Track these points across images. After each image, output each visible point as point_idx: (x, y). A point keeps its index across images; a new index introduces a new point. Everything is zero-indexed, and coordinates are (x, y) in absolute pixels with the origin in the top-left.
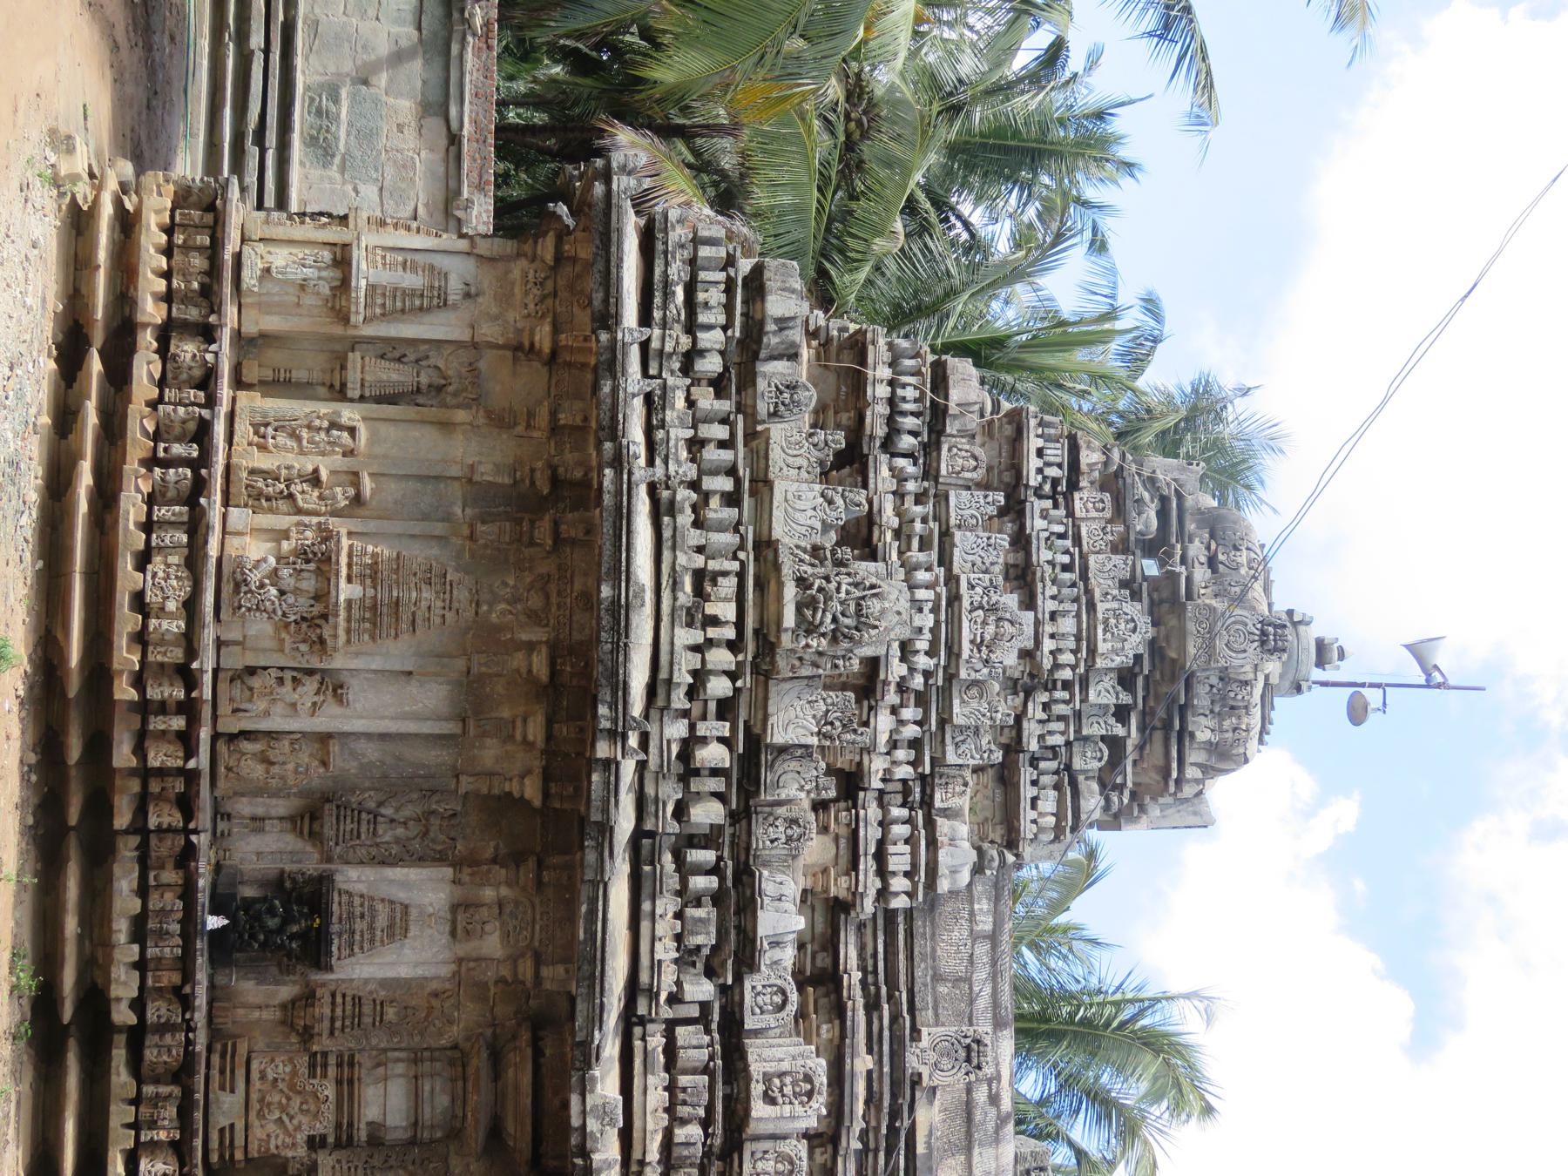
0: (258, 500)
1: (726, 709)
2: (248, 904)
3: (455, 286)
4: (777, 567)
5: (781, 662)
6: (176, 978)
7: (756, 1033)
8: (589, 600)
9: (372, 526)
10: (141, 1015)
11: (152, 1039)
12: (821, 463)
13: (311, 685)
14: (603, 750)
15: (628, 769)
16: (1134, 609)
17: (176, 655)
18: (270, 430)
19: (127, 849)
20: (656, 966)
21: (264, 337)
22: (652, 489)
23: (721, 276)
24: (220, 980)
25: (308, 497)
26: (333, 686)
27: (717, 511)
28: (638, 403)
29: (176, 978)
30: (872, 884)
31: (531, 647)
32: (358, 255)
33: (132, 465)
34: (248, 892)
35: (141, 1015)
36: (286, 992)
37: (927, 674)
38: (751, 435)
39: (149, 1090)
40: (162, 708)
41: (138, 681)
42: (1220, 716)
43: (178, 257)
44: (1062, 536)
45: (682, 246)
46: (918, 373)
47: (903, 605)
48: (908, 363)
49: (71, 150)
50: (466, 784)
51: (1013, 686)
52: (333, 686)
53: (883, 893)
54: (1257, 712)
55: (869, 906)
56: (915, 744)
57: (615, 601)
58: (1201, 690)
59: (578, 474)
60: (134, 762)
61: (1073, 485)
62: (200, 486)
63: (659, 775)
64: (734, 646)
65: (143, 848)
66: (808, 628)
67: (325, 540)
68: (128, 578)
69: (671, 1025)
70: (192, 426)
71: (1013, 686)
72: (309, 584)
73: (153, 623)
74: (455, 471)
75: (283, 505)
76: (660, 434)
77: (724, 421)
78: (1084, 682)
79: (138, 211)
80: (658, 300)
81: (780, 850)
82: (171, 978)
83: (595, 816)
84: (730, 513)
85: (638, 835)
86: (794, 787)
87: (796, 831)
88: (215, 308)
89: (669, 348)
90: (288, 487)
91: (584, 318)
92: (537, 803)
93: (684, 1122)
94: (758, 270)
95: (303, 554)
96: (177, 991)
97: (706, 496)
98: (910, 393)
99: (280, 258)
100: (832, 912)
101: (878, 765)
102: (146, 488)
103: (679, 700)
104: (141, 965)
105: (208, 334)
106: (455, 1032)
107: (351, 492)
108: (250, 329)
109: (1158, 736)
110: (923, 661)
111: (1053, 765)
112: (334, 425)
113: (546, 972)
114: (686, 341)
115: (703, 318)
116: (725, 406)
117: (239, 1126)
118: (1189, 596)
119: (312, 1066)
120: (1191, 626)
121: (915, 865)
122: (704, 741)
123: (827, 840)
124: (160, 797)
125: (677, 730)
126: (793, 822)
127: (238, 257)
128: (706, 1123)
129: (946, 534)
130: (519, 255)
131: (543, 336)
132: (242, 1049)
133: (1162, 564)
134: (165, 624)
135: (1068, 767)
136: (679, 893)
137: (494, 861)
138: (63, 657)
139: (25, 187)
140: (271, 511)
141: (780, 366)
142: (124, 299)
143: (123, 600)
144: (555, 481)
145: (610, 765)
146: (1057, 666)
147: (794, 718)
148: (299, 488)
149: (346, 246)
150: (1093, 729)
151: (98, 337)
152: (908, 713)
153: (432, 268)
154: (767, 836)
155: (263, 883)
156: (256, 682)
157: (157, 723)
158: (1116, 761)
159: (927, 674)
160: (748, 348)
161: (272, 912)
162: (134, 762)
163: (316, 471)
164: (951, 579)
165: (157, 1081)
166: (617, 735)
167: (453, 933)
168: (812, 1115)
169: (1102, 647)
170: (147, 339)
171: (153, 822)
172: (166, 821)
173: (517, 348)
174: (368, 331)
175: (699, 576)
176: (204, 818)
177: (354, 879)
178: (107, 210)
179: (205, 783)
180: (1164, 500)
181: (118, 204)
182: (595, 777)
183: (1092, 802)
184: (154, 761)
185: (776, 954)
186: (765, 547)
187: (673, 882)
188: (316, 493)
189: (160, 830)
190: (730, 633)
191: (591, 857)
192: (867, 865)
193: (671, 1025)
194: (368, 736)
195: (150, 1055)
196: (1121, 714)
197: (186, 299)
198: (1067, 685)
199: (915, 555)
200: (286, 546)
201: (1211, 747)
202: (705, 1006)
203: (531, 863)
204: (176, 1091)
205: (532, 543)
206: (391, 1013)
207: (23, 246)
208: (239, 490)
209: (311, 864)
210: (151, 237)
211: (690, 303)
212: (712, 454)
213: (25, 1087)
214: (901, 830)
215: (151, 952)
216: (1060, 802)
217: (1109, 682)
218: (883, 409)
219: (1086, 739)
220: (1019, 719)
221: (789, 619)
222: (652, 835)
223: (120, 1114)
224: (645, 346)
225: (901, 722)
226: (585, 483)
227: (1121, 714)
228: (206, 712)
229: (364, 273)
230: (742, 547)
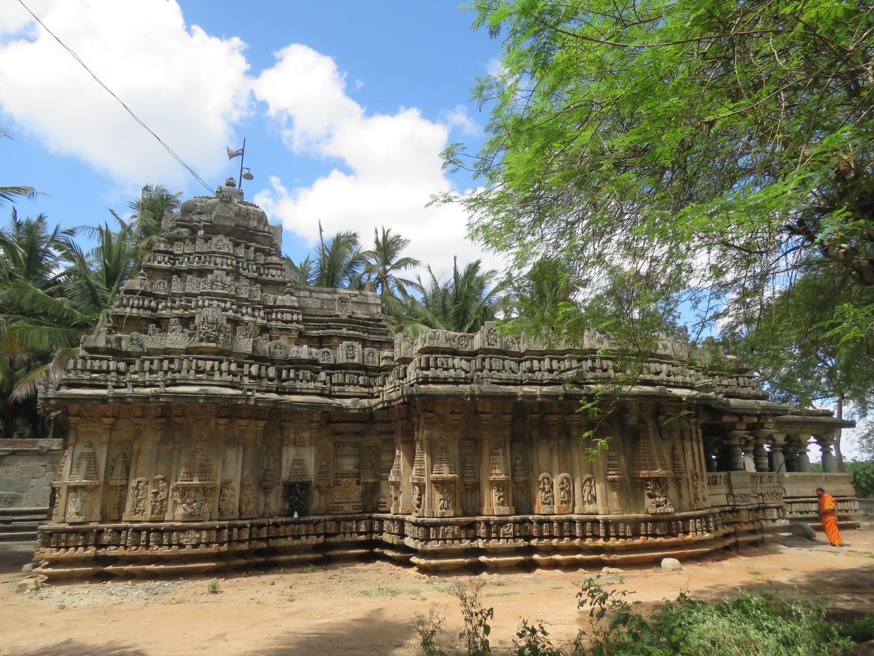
1: (240, 365)
2: (291, 506)
3: (87, 450)
4: (196, 348)
5: (227, 348)
6: (312, 525)
7: (335, 360)
8: (203, 406)
9: (174, 474)
10: (321, 534)
11: (328, 531)
12: (160, 332)
13: (226, 491)
14: (252, 402)
15: (258, 395)
16: (215, 240)
17: (214, 533)
19: (272, 543)
20: (316, 388)
21: (102, 513)
22: (167, 386)
23: (89, 362)
24: (312, 513)
25: (162, 495)
26: (226, 484)
27: (175, 366)
28: (136, 390)
29: (312, 525)
30: (295, 324)
31: (217, 424)
32: (72, 483)
33: (148, 552)
34: (287, 506)
35: (321, 534)
36: (316, 494)
37: (232, 304)
38: (148, 354)
39: (342, 531)
40: (230, 536)
41: (221, 544)
42: (250, 218)
43: (70, 544)
44: (189, 259)
45: (77, 374)
46: (129, 299)
47: (210, 309)
48: (125, 302)
49: (25, 585)
50: (259, 443)
51: (237, 279)
52: (226, 484)
53: (298, 322)
54: (249, 207)
55: (301, 326)
56: (254, 309)
57: (205, 398)
58: (241, 222)
59: (159, 409)
60: (247, 543)
61: (172, 253)
62: (157, 530)
63: (260, 386)
64: (221, 362)
65: (273, 538)
66: (216, 340)
67: (178, 489)
69: (332, 384)
70: (135, 534)
71: (237, 279)
72: (193, 493)
73: (203, 541)
74: (156, 448)
76: (147, 383)
77: (143, 362)
78: (237, 257)
79: (47, 560)
80: (97, 383)
81: (283, 351)
82: (311, 527)
83: (272, 405)
84: (176, 362)
85: (277, 392)
86: (265, 346)
88: (91, 530)
89: (115, 379)
91: (102, 407)
92: (266, 422)
93: (358, 381)
94: (87, 349)
95: (182, 496)
96: (315, 525)
97: (170, 369)
98: (136, 302)
99: (72, 509)
100: (302, 338)
101: (260, 321)
102: (156, 547)
103: (237, 379)
104: (307, 536)
105: (100, 532)
106: (330, 445)
108: (99, 518)
109: (255, 238)
110: (228, 305)
111: (262, 270)
112: (137, 488)
113: (315, 420)
114: (113, 374)
115: (105, 367)
116: (138, 362)
118: (211, 222)
119: (337, 485)
120: (221, 223)
121: (290, 312)
122: (250, 372)
123: (281, 337)
124: (258, 534)
125: (246, 380)
126: (275, 347)
127: (71, 524)
128: (359, 375)
129: (186, 295)
130: (76, 429)
131: (108, 421)
132: (331, 505)
133: (200, 229)
134: (204, 537)
135: (263, 265)
136: (295, 381)
137: (282, 435)
138: (213, 567)
139: (42, 599)
140: (166, 507)
141: (123, 343)
142: (84, 561)
143: (195, 551)
144: (161, 417)
145: (257, 400)
146: (232, 265)
147: (245, 345)
149: (69, 487)
150: (252, 256)
151: (99, 568)
152: (244, 311)
153: (79, 458)
154: (279, 355)
155: (285, 502)
156: (223, 508)
157: (235, 537)
158: (262, 251)
159: (232, 304)
160: (117, 354)
161: (293, 499)
162: (247, 543)
164: (202, 294)
165: (339, 529)
166: (248, 398)
168: (358, 346)
169: (226, 250)
170: (101, 552)
171: (265, 536)
172: (265, 532)
173: (111, 429)
174: (102, 478)
175: (198, 371)
176: (265, 521)
177: (285, 475)
178: (50, 570)
179: (254, 521)
180: (178, 225)
181: (46, 567)
183: (274, 259)
184: (247, 536)
185: (314, 354)
186: (188, 351)
187: (292, 382)
189: (268, 533)
190: (217, 363)
191: (283, 406)
192: (289, 326)
193: (332, 384)
194: (242, 472)
195: (332, 531)
196: (247, 247)
197: (86, 540)
198: (238, 263)
199: (193, 305)
200: (179, 501)
202: (327, 374)
203: (283, 424)
204: (342, 523)
205: (182, 424)
206: (324, 463)
207: (65, 596)
209: (280, 488)
210: (62, 553)
211: (99, 372)
212: (155, 366)
213: (339, 565)
215: (304, 533)
216: (273, 268)
217: (237, 250)
218: (141, 311)
219: (255, 258)
220: (247, 278)
221: (214, 345)
222: (277, 388)
223: (348, 538)
224: (115, 387)
225: (247, 313)
226: (163, 407)
227: (247, 247)
228: (232, 522)
229: (79, 480)
230: (188, 358)
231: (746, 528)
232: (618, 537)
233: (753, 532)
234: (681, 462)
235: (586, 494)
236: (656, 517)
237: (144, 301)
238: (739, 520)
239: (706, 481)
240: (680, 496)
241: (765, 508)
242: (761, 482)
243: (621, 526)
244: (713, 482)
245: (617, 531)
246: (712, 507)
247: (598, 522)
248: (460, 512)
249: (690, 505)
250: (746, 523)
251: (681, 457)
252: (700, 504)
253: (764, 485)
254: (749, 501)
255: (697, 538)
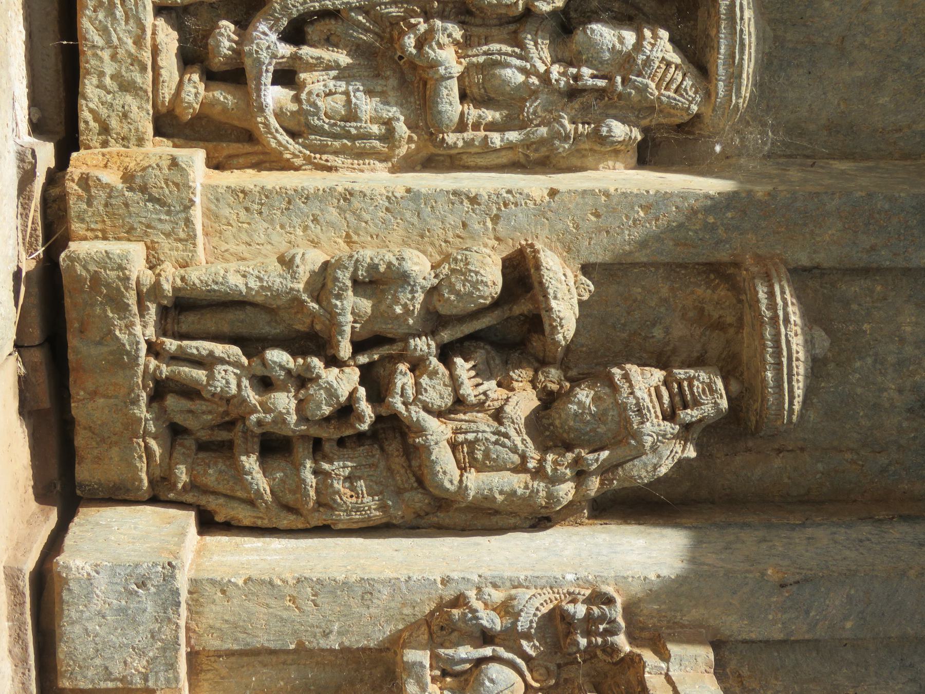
0: (215, 464)
18: (268, 43)
75: (346, 483)
90: (376, 383)
107: (712, 395)
148: (437, 392)
163: (521, 273)
188: (523, 402)
208: (125, 426)
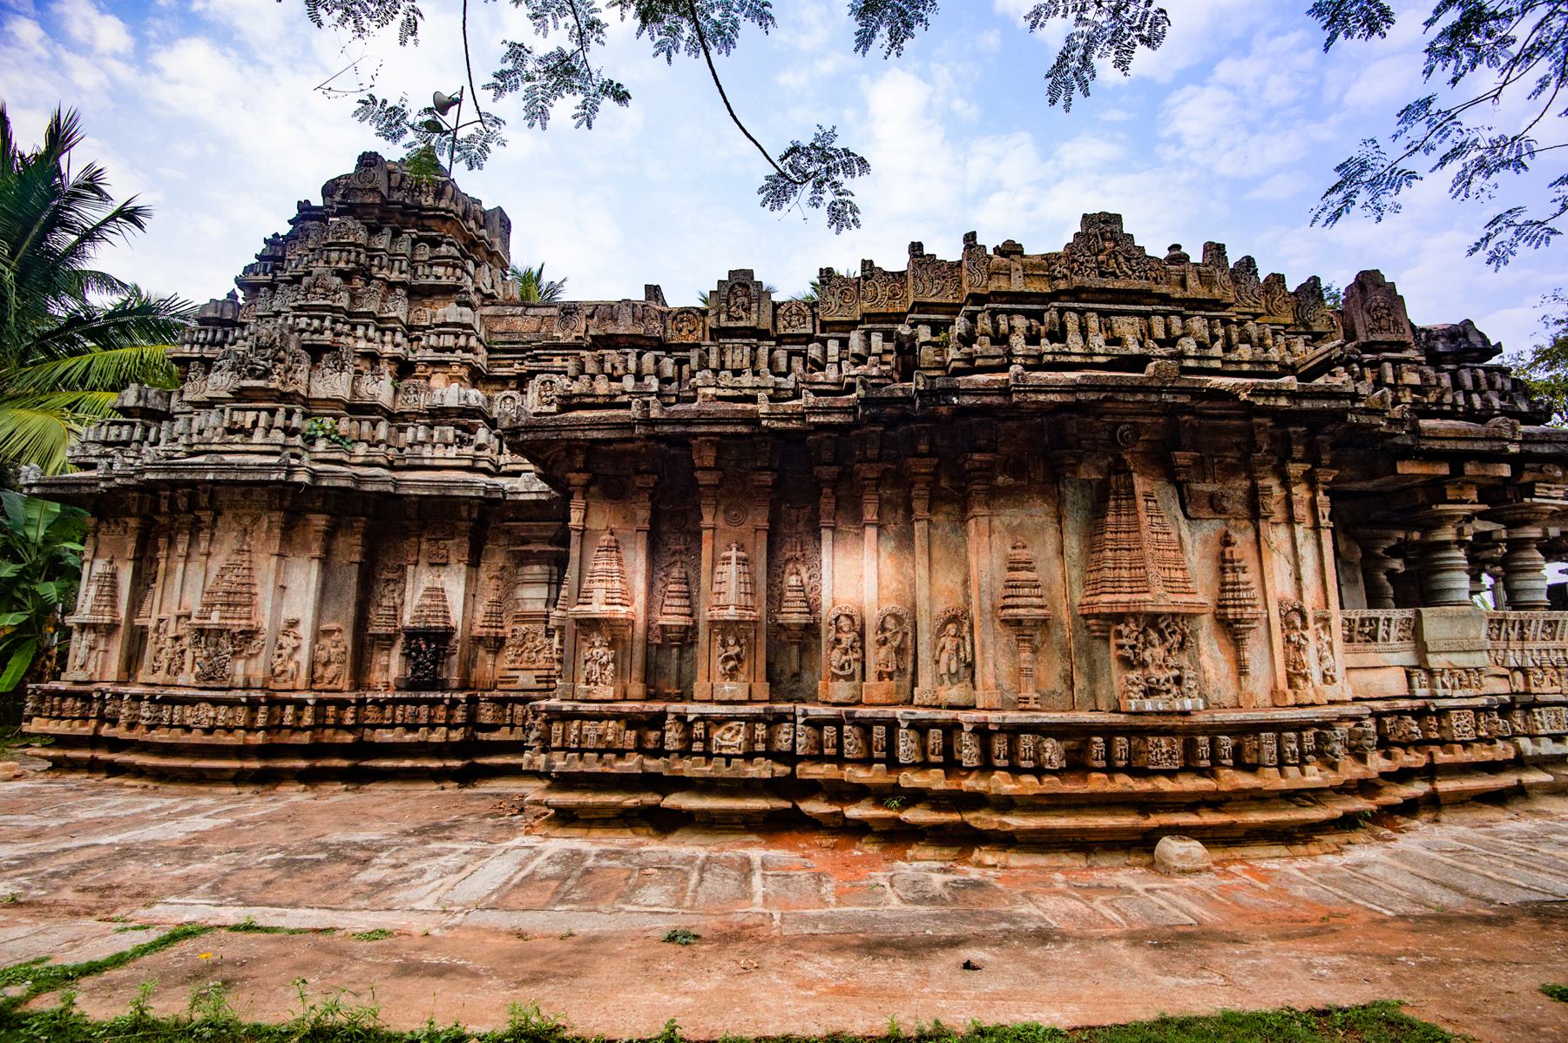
42: (421, 192)
66: (266, 374)
68: (196, 737)
87: (412, 390)
115: (124, 437)
117: (537, 673)
143: (207, 739)
167: (445, 565)
182: (325, 483)
192: (446, 356)
196: (396, 234)
201: (439, 195)
214: (433, 340)
221: (261, 383)
231: (1462, 756)
232: (1015, 770)
233: (1493, 767)
234: (1250, 576)
235: (944, 658)
236: (1138, 721)
237: (215, 332)
238: (1446, 734)
239: (1338, 632)
240: (1241, 670)
241: (1531, 705)
242: (1522, 638)
243: (1026, 741)
244: (1363, 634)
245: (1012, 754)
246: (1356, 699)
247: (957, 726)
248: (637, 689)
249: (1274, 692)
250: (1466, 745)
251: (1252, 565)
252: (1308, 693)
253: (1527, 645)
254: (1480, 685)
255: (1283, 784)
